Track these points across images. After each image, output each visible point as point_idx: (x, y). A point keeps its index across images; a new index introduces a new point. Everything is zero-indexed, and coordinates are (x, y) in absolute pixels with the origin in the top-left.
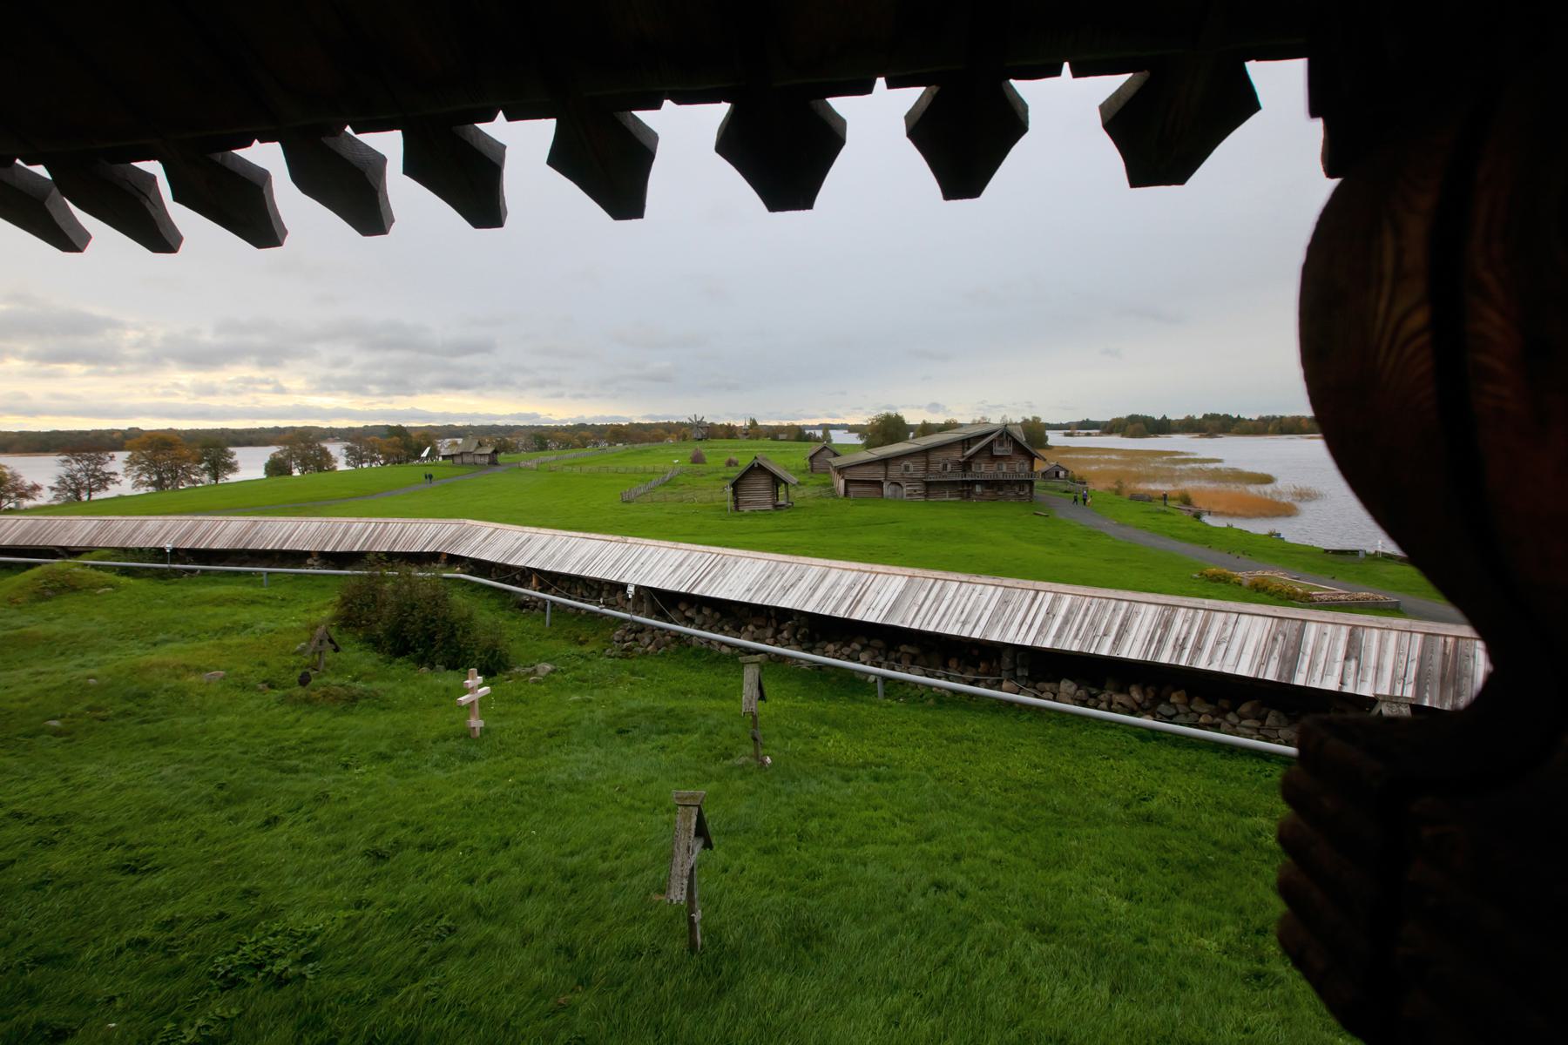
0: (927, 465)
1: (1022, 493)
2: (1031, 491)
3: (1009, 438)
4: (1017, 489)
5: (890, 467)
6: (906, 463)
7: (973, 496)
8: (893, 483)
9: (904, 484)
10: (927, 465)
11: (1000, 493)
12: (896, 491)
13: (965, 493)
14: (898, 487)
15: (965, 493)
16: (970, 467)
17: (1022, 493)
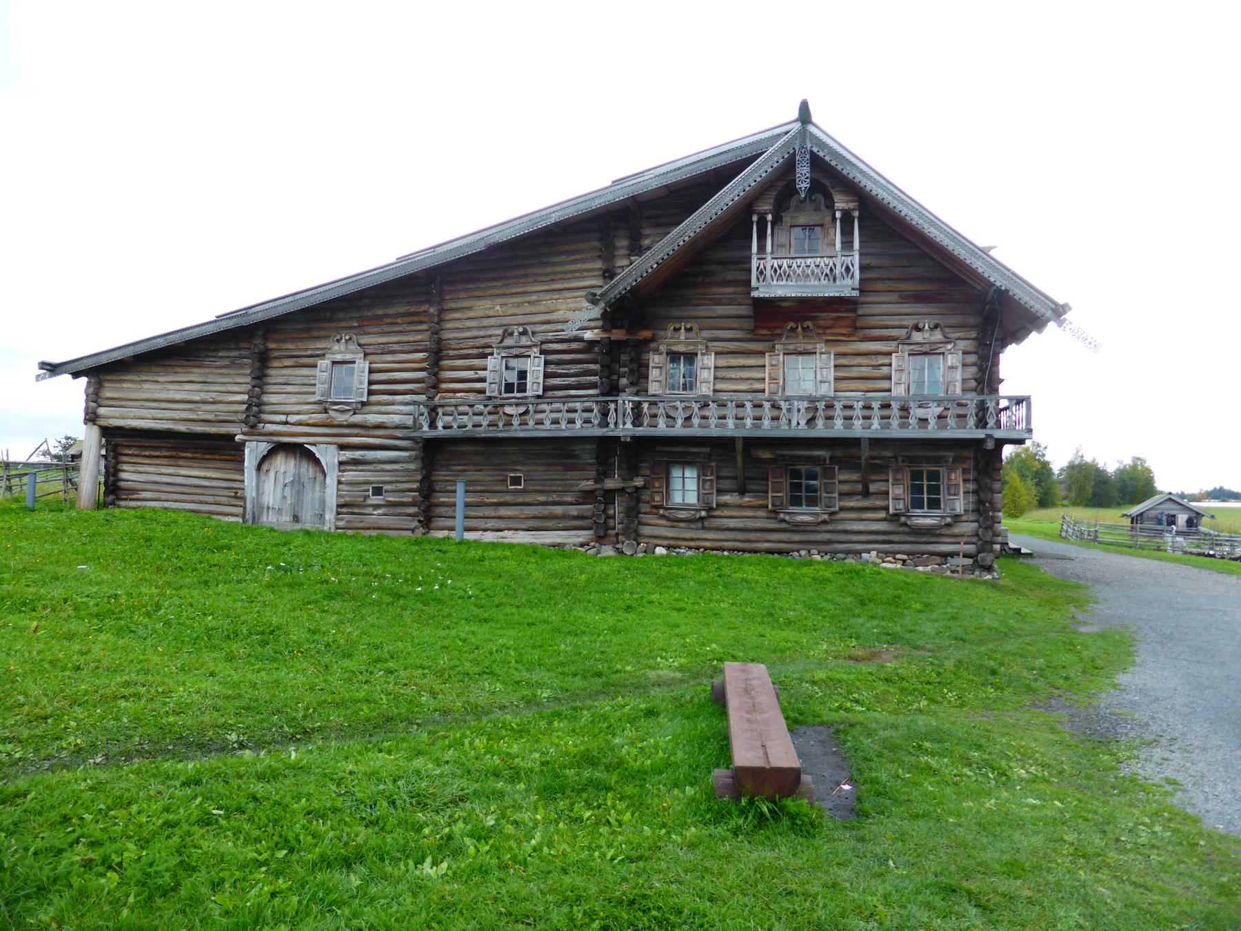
0: (437, 355)
1: (925, 519)
2: (984, 510)
3: (841, 203)
4: (897, 493)
5: (276, 374)
6: (339, 350)
7: (654, 527)
8: (279, 448)
9: (329, 456)
10: (437, 355)
11: (803, 515)
12: (297, 484)
13: (617, 509)
14: (307, 470)
15: (617, 509)
16: (640, 375)
17: (925, 519)
